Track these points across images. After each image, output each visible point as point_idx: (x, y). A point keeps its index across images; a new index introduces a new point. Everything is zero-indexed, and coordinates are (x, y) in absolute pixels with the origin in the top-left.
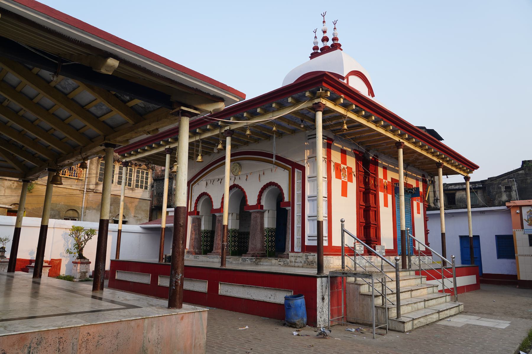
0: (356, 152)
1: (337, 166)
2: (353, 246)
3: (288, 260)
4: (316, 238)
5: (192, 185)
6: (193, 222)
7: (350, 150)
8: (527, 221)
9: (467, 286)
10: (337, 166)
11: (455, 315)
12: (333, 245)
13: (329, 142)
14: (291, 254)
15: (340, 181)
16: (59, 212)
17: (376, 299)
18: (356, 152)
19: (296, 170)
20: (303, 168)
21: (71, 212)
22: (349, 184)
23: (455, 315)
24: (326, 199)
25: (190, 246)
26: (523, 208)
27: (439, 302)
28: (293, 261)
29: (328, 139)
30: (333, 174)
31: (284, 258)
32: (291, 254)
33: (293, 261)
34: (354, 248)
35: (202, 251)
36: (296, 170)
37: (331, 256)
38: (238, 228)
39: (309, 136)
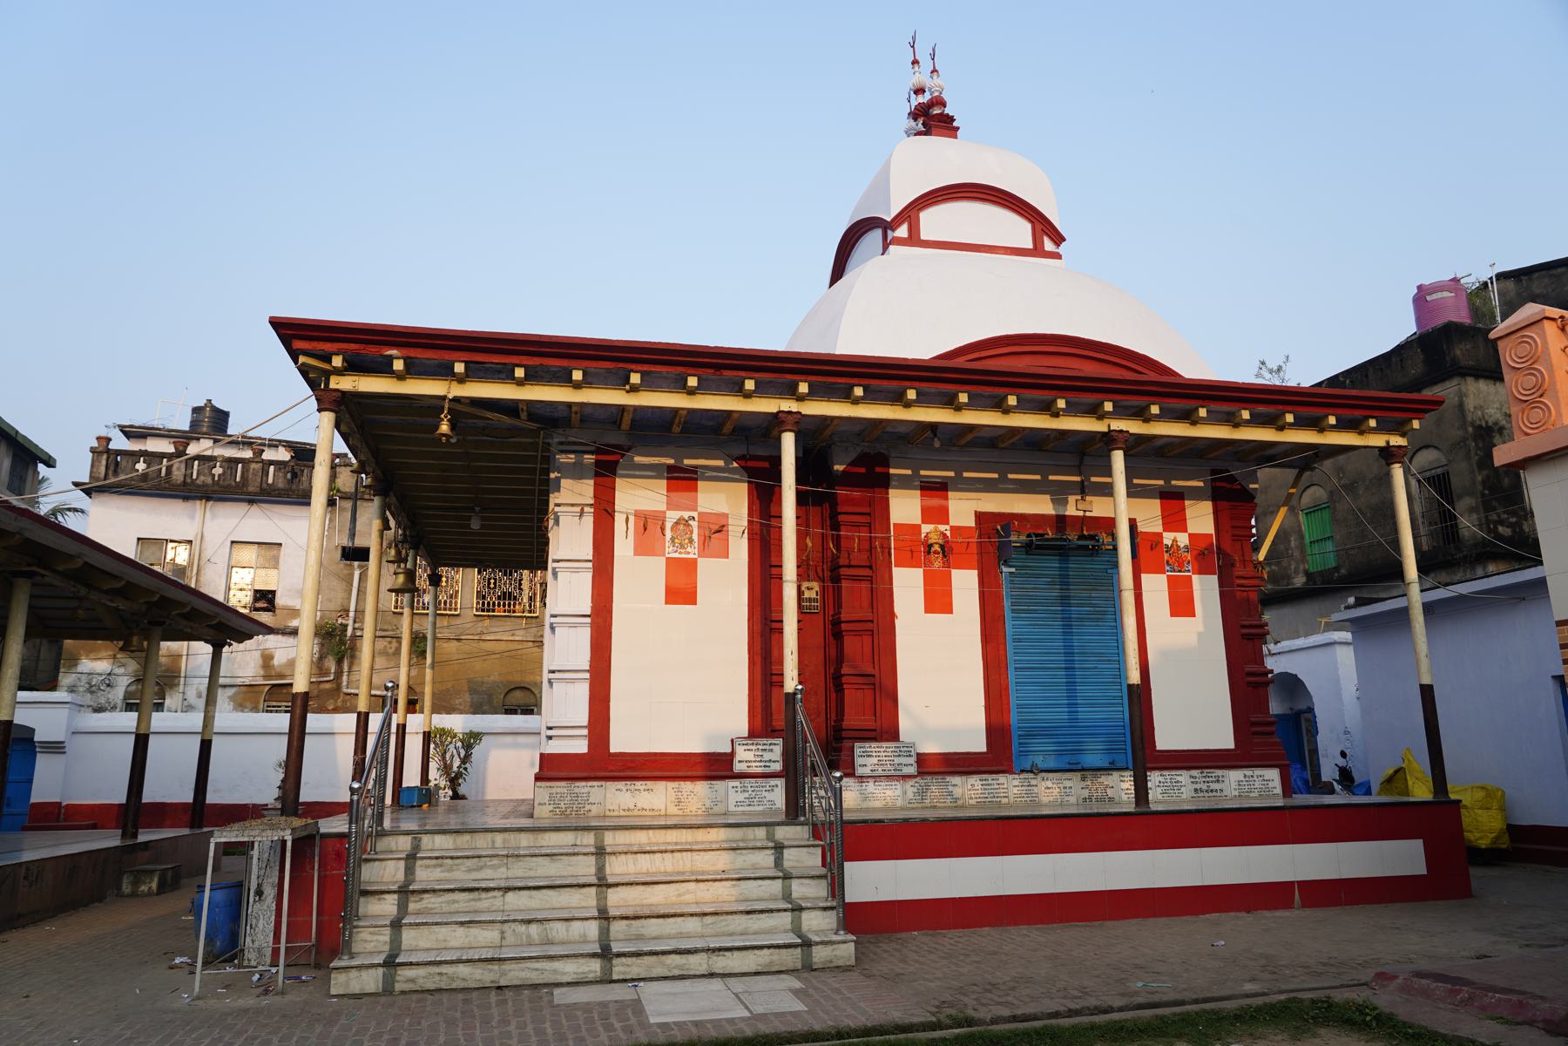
0: (750, 464)
1: (647, 524)
2: (729, 750)
7: (721, 463)
9: (1303, 885)
10: (647, 524)
11: (757, 973)
12: (614, 748)
13: (601, 457)
15: (660, 563)
16: (490, 696)
17: (362, 900)
18: (750, 464)
21: (518, 694)
22: (706, 567)
23: (757, 973)
24: (588, 620)
27: (731, 928)
29: (597, 452)
30: (623, 544)
34: (732, 754)
37: (595, 783)
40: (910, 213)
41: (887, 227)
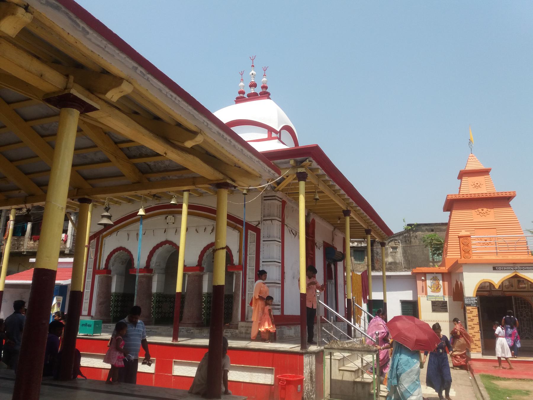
3: (237, 331)
4: (280, 307)
5: (103, 237)
6: (101, 283)
8: (431, 288)
14: (241, 324)
19: (250, 231)
20: (257, 230)
25: (96, 313)
26: (427, 275)
28: (244, 332)
31: (231, 328)
32: (241, 324)
33: (244, 332)
35: (112, 318)
36: (250, 231)
38: (162, 291)
39: (265, 197)
40: (280, 132)
41: (270, 130)
